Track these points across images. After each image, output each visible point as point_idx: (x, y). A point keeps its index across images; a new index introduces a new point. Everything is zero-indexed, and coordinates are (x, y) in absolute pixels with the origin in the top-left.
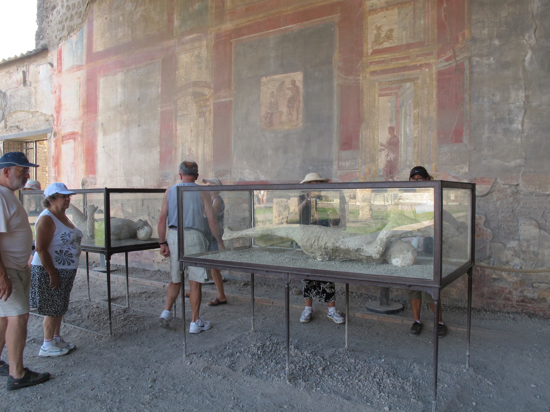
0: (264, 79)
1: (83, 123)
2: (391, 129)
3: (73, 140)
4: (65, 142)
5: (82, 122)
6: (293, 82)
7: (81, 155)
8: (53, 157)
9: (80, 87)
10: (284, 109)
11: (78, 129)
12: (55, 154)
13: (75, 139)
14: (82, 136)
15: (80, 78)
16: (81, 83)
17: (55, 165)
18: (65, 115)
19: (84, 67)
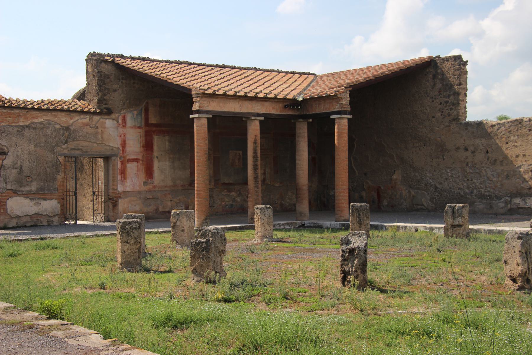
0: (230, 151)
1: (143, 155)
2: (264, 170)
3: (136, 163)
4: (129, 162)
5: (142, 154)
6: (239, 154)
7: (142, 170)
8: (120, 170)
9: (140, 137)
10: (237, 161)
11: (140, 157)
12: (121, 168)
13: (138, 162)
14: (142, 161)
15: (140, 133)
16: (141, 136)
17: (121, 174)
18: (128, 149)
19: (143, 128)
